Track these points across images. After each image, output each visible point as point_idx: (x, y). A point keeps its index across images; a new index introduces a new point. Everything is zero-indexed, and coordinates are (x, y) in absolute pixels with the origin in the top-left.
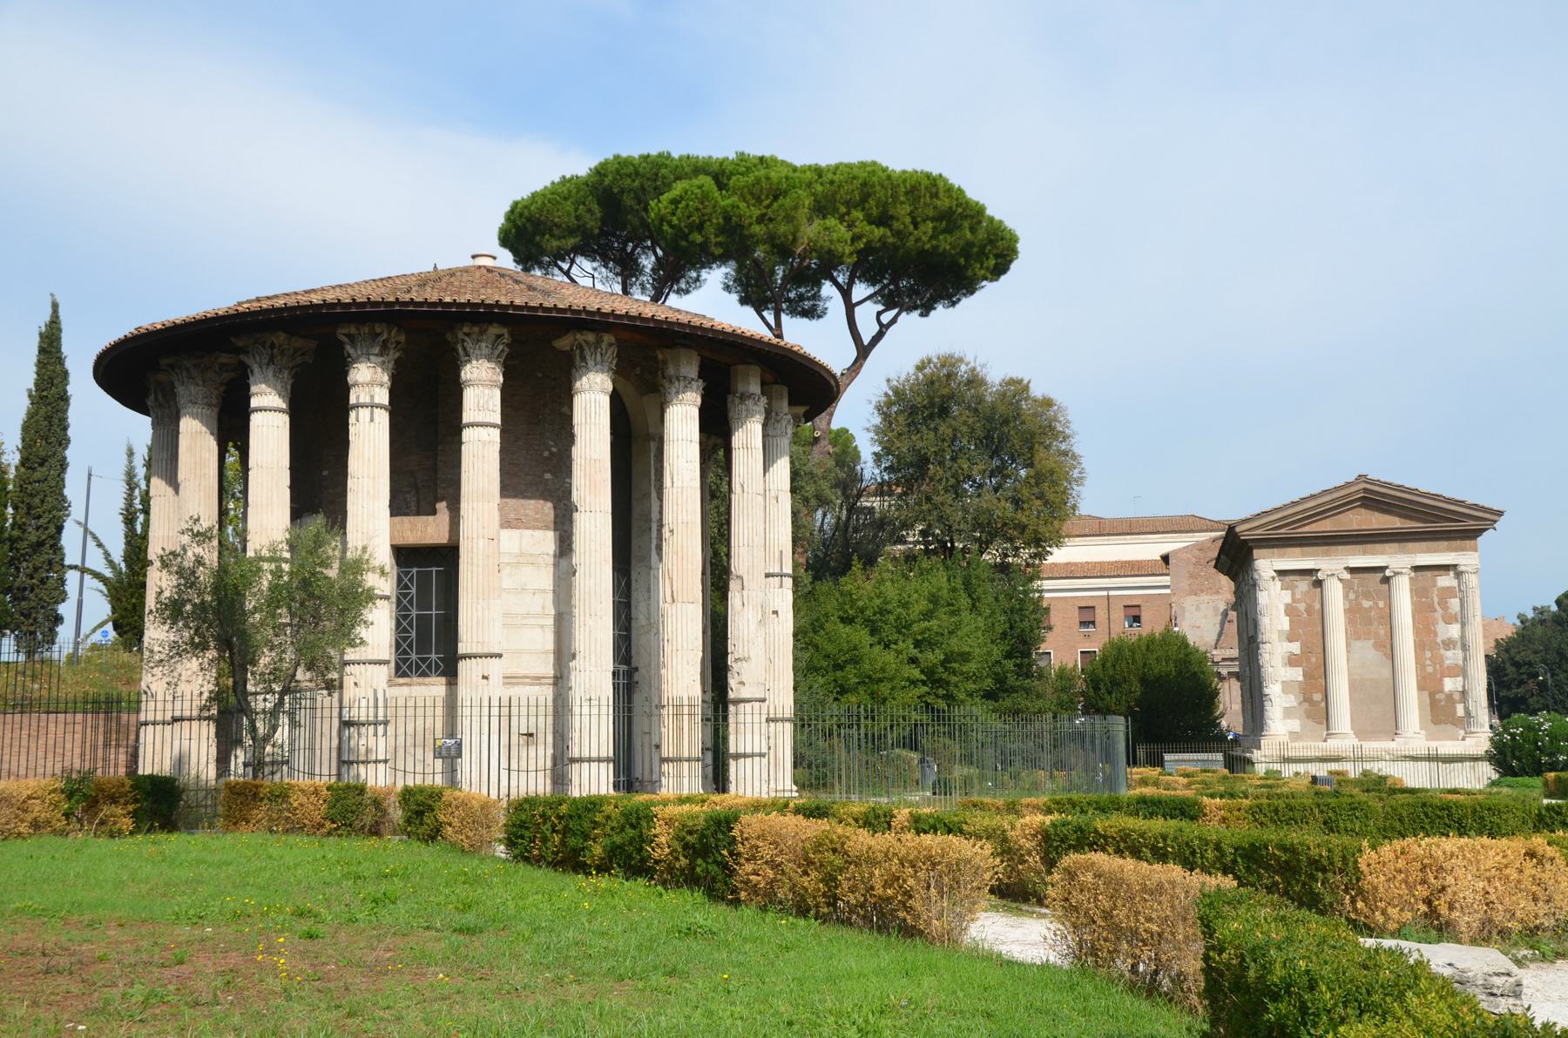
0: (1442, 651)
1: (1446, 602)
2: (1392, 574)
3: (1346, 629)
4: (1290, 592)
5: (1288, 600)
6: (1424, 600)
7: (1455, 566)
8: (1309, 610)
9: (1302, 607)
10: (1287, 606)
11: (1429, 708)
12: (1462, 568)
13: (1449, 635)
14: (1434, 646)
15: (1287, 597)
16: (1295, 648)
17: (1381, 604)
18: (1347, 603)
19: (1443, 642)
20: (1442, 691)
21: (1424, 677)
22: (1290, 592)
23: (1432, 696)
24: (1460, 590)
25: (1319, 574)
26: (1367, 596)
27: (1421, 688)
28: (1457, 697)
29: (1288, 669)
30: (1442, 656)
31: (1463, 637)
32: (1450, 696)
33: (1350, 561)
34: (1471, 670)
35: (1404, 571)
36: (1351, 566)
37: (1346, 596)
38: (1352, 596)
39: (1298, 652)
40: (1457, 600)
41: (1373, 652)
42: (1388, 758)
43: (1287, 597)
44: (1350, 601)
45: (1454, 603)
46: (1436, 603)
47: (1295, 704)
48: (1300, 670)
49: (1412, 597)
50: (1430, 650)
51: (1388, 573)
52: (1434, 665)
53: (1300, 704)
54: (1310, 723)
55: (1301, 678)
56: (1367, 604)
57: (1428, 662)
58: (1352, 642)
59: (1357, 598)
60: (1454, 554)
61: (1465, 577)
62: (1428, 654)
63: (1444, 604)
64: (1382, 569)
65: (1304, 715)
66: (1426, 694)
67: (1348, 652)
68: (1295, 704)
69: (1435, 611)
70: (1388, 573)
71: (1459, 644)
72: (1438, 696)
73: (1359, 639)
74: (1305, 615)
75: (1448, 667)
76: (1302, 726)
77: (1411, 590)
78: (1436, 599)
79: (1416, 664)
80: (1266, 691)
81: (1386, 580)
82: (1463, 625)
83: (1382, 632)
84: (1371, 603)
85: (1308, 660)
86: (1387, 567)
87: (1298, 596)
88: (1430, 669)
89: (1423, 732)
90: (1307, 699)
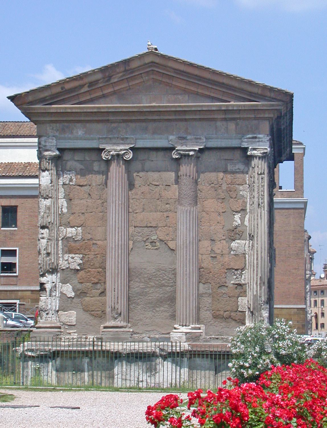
61: (255, 162)
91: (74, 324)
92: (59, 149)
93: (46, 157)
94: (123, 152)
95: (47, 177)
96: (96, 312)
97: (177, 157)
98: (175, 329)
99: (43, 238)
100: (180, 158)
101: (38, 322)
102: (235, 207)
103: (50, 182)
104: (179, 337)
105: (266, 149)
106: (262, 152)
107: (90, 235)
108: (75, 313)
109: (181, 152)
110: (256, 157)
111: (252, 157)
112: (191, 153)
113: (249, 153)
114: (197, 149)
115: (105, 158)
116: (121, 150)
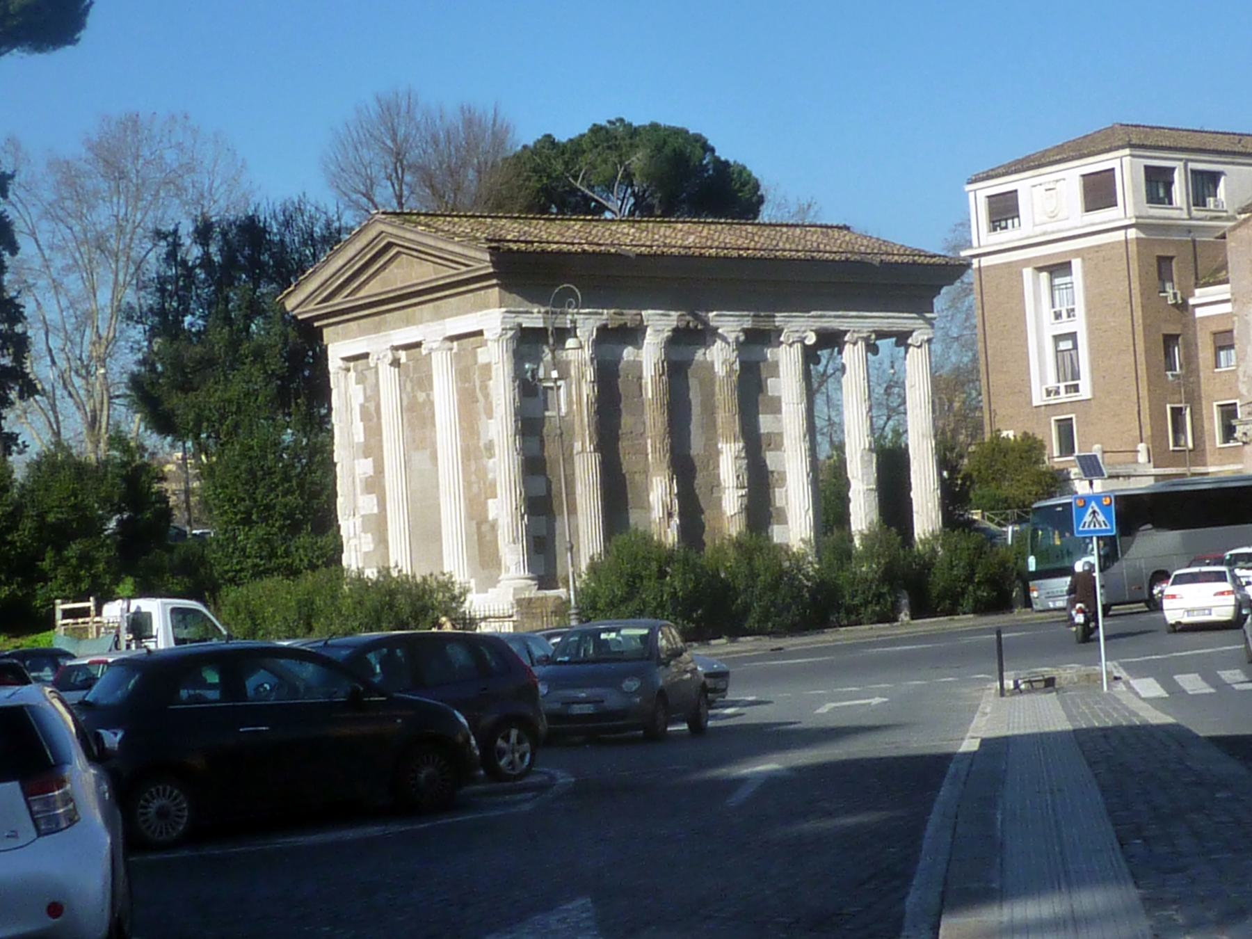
0: (485, 459)
4: (360, 387)
5: (361, 400)
9: (372, 406)
10: (362, 406)
18: (404, 396)
20: (486, 520)
35: (435, 345)
46: (478, 390)
57: (473, 478)
59: (413, 389)
60: (479, 314)
66: (474, 523)
73: (417, 449)
78: (478, 384)
84: (424, 395)
114: (441, 338)
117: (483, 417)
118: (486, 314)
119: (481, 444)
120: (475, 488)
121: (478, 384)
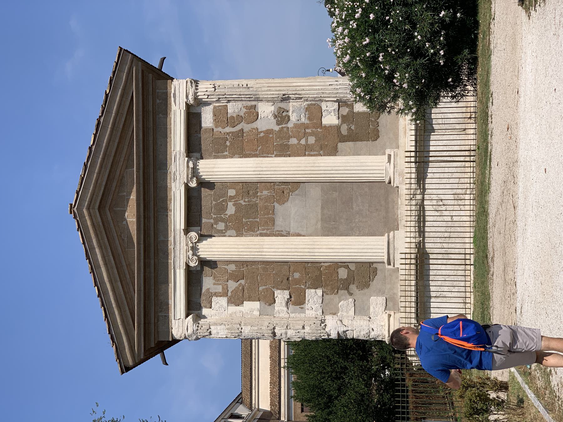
0: (290, 125)
1: (232, 117)
2: (195, 179)
3: (262, 235)
4: (214, 299)
5: (223, 301)
6: (228, 143)
7: (188, 106)
8: (236, 277)
9: (232, 285)
11: (359, 143)
12: (191, 101)
13: (271, 116)
14: (284, 134)
15: (220, 302)
16: (281, 296)
17: (232, 192)
18: (229, 232)
19: (278, 124)
20: (338, 128)
21: (321, 148)
22: (214, 299)
23: (344, 139)
24: (218, 101)
25: (192, 264)
26: (222, 208)
27: (334, 152)
28: (345, 111)
29: (307, 306)
30: (296, 126)
31: (273, 101)
32: (344, 119)
33: (178, 227)
34: (313, 94)
36: (183, 227)
37: (222, 233)
38: (221, 226)
39: (287, 293)
40: (230, 105)
41: (288, 204)
42: (419, 197)
43: (220, 302)
44: (227, 228)
45: (233, 109)
47: (350, 300)
48: (310, 293)
49: (225, 157)
50: (290, 137)
51: (193, 184)
52: (305, 135)
53: (351, 294)
54: (375, 284)
55: (320, 292)
56: (231, 210)
57: (303, 142)
58: (277, 228)
59: (223, 220)
61: (201, 95)
62: (293, 141)
63: (233, 121)
64: (188, 189)
65: (366, 290)
67: (288, 234)
68: (350, 300)
69: (242, 130)
70: (193, 184)
71: (283, 105)
72: (344, 130)
73: (273, 221)
74: (243, 282)
75: (309, 119)
76: (380, 292)
77: (216, 157)
78: (228, 129)
79: (305, 155)
80: (334, 336)
81: (204, 184)
82: (258, 100)
83: (265, 192)
84: (230, 204)
85: (298, 282)
86: (187, 186)
87: (219, 289)
88: (312, 140)
89: (388, 151)
90: (345, 285)
91: (385, 299)
92: (187, 316)
93: (195, 330)
94: (190, 242)
95: (218, 329)
96: (371, 274)
97: (195, 182)
98: (390, 183)
99: (286, 333)
100: (197, 178)
101: (383, 340)
102: (252, 117)
103: (223, 326)
104: (399, 175)
105: (187, 82)
106: (190, 86)
107: (284, 281)
108: (372, 297)
109: (190, 176)
110: (196, 93)
111: (196, 98)
112: (191, 165)
113: (192, 102)
114: (186, 159)
115: (195, 263)
116: (187, 245)
117: (254, 125)
118: (175, 94)
119: (277, 128)
120: (312, 140)
121: (228, 129)
